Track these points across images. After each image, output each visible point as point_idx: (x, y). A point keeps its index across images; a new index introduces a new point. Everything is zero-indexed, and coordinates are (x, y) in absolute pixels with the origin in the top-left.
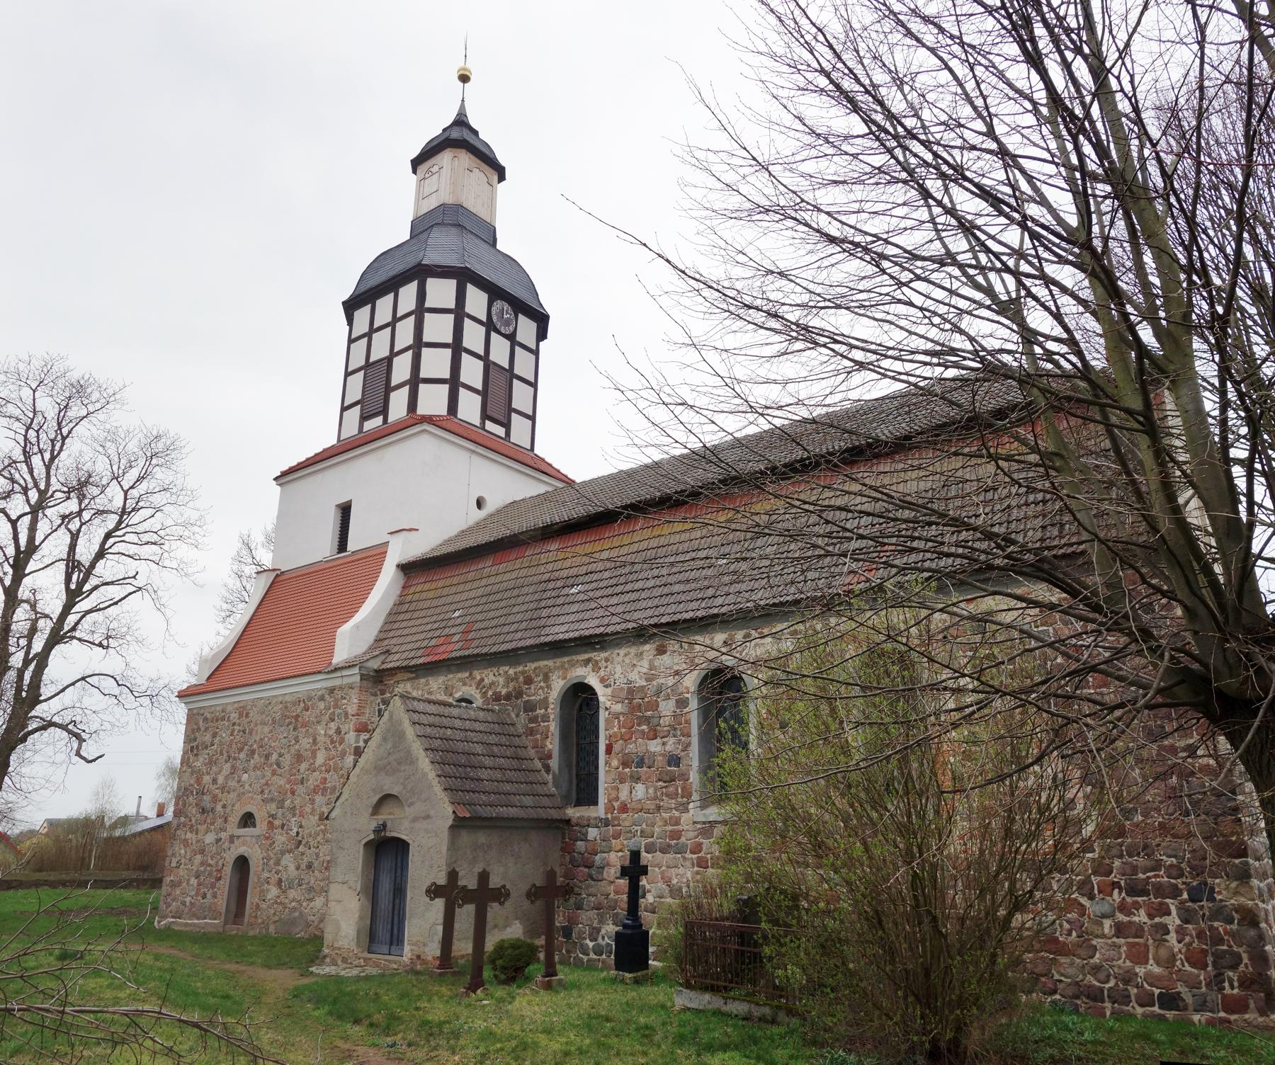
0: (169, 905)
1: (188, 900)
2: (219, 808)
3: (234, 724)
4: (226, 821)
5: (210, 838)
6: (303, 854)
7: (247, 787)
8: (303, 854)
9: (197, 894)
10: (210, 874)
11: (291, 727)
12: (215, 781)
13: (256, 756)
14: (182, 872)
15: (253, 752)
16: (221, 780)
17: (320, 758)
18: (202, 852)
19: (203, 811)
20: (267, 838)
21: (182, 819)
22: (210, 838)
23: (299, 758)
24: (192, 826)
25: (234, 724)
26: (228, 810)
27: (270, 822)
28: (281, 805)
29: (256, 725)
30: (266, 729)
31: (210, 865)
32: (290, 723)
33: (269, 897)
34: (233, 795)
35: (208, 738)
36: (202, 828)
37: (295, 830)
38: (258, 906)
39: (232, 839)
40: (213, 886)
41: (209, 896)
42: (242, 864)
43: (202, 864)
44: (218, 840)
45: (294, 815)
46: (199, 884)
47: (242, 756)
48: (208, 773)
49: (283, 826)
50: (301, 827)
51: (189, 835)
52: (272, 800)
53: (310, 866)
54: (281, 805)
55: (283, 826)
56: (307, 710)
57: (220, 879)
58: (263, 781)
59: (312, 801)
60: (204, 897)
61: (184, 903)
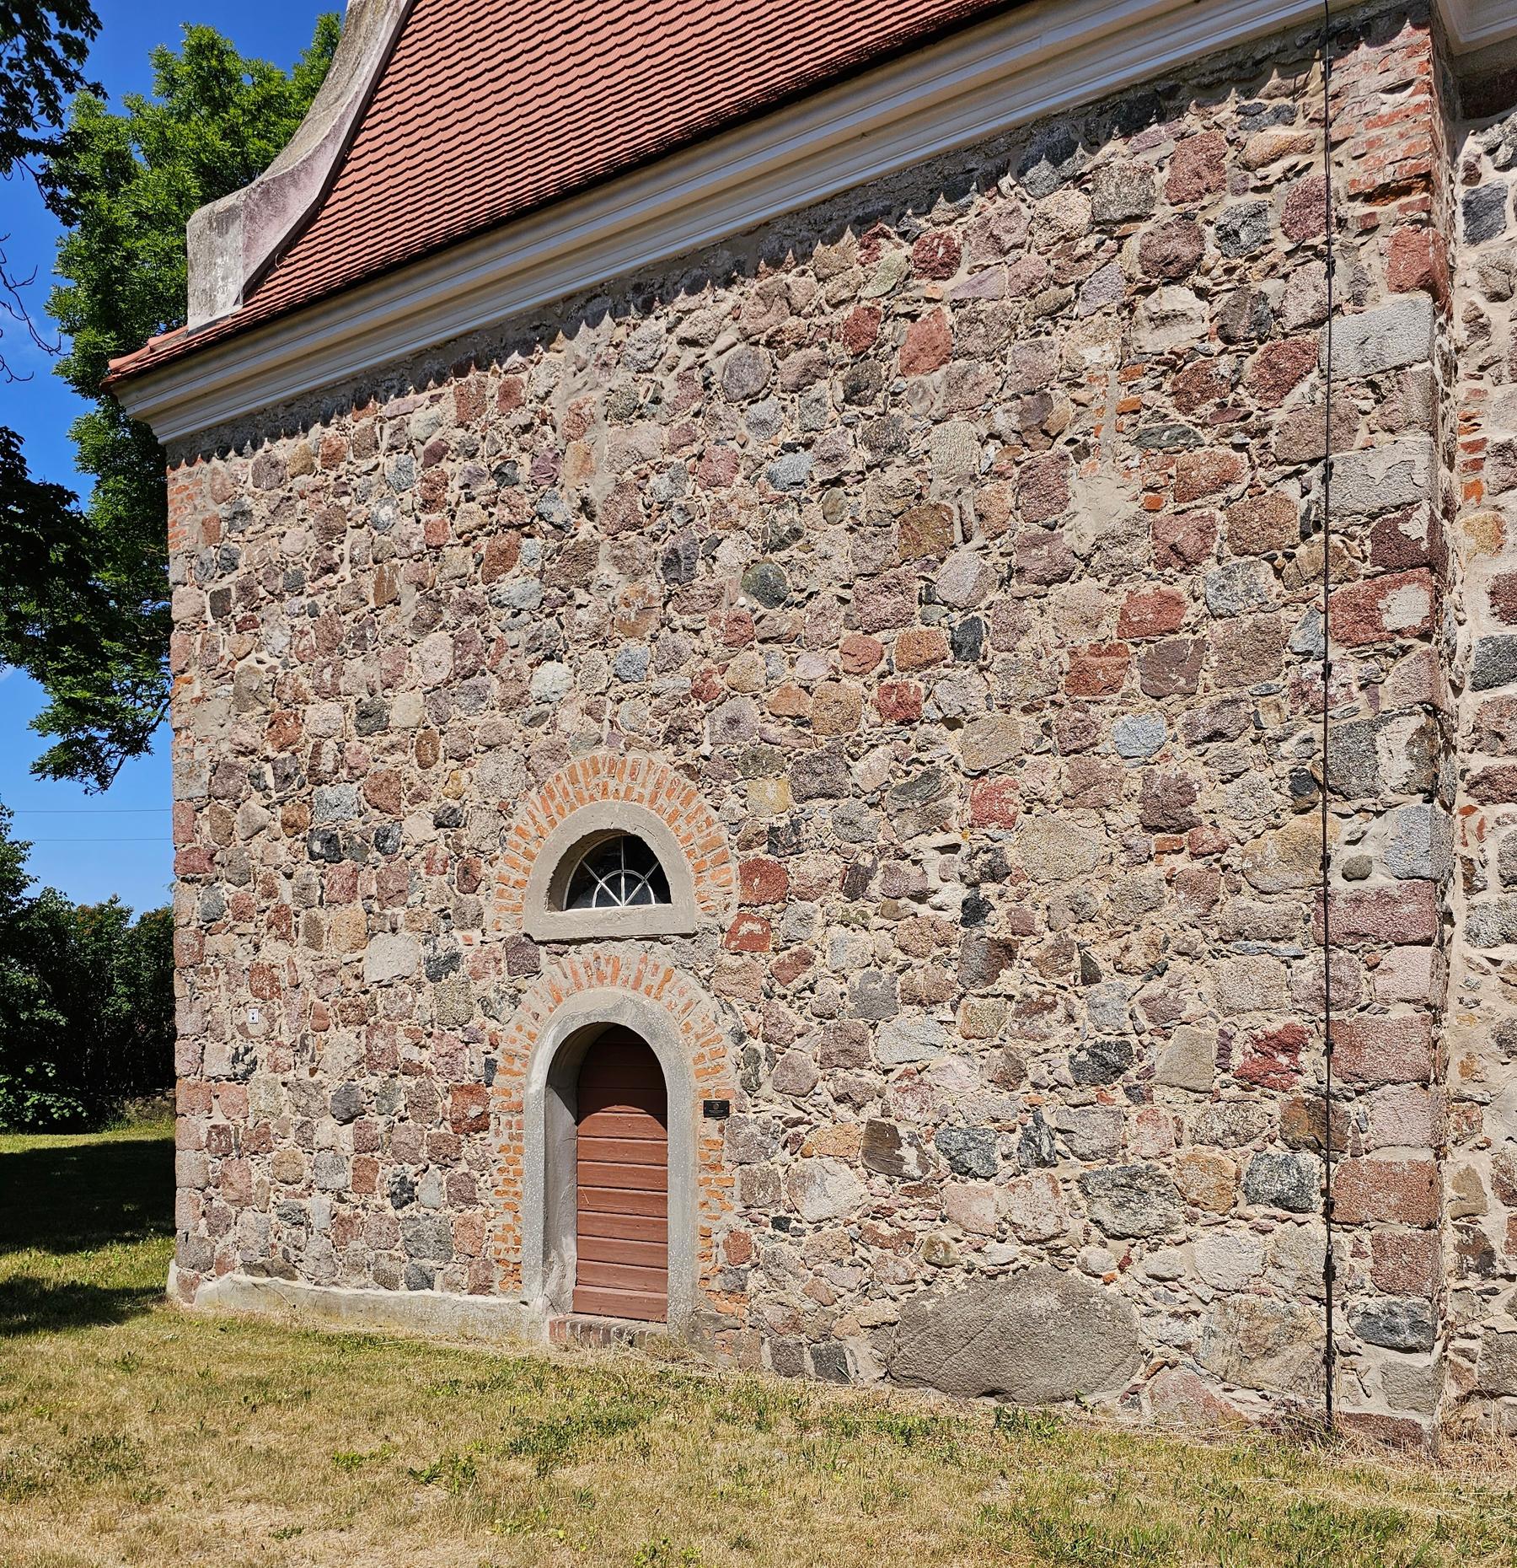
0: (219, 1224)
1: (318, 1206)
2: (418, 826)
3: (436, 455)
4: (469, 880)
5: (392, 957)
6: (1034, 1008)
7: (570, 719)
8: (1034, 1008)
9: (363, 1182)
10: (420, 1105)
11: (830, 389)
12: (371, 718)
13: (605, 571)
14: (262, 1093)
15: (584, 557)
16: (405, 708)
17: (1101, 499)
18: (360, 1016)
19: (333, 849)
20: (753, 943)
21: (227, 891)
22: (392, 957)
23: (921, 525)
24: (282, 913)
25: (436, 455)
26: (469, 836)
27: (749, 871)
28: (819, 779)
29: (581, 422)
30: (648, 435)
31: (411, 1069)
32: (810, 376)
33: (812, 1207)
34: (486, 766)
35: (297, 539)
36: (345, 918)
37: (953, 895)
38: (738, 1246)
39: (522, 954)
40: (444, 1157)
41: (431, 1189)
42: (608, 1069)
43: (369, 1062)
44: (441, 967)
45: (935, 821)
46: (365, 1146)
47: (511, 586)
48: (329, 693)
49: (855, 883)
50: (995, 873)
51: (273, 951)
52: (754, 763)
53: (1104, 1065)
54: (819, 779)
55: (855, 883)
56: (944, 268)
57: (480, 1124)
58: (678, 682)
59: (1078, 744)
60: (404, 1194)
61: (299, 1219)
